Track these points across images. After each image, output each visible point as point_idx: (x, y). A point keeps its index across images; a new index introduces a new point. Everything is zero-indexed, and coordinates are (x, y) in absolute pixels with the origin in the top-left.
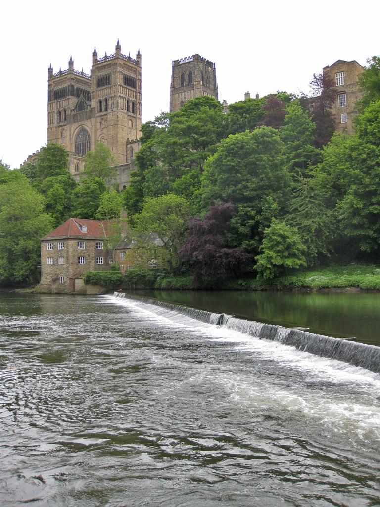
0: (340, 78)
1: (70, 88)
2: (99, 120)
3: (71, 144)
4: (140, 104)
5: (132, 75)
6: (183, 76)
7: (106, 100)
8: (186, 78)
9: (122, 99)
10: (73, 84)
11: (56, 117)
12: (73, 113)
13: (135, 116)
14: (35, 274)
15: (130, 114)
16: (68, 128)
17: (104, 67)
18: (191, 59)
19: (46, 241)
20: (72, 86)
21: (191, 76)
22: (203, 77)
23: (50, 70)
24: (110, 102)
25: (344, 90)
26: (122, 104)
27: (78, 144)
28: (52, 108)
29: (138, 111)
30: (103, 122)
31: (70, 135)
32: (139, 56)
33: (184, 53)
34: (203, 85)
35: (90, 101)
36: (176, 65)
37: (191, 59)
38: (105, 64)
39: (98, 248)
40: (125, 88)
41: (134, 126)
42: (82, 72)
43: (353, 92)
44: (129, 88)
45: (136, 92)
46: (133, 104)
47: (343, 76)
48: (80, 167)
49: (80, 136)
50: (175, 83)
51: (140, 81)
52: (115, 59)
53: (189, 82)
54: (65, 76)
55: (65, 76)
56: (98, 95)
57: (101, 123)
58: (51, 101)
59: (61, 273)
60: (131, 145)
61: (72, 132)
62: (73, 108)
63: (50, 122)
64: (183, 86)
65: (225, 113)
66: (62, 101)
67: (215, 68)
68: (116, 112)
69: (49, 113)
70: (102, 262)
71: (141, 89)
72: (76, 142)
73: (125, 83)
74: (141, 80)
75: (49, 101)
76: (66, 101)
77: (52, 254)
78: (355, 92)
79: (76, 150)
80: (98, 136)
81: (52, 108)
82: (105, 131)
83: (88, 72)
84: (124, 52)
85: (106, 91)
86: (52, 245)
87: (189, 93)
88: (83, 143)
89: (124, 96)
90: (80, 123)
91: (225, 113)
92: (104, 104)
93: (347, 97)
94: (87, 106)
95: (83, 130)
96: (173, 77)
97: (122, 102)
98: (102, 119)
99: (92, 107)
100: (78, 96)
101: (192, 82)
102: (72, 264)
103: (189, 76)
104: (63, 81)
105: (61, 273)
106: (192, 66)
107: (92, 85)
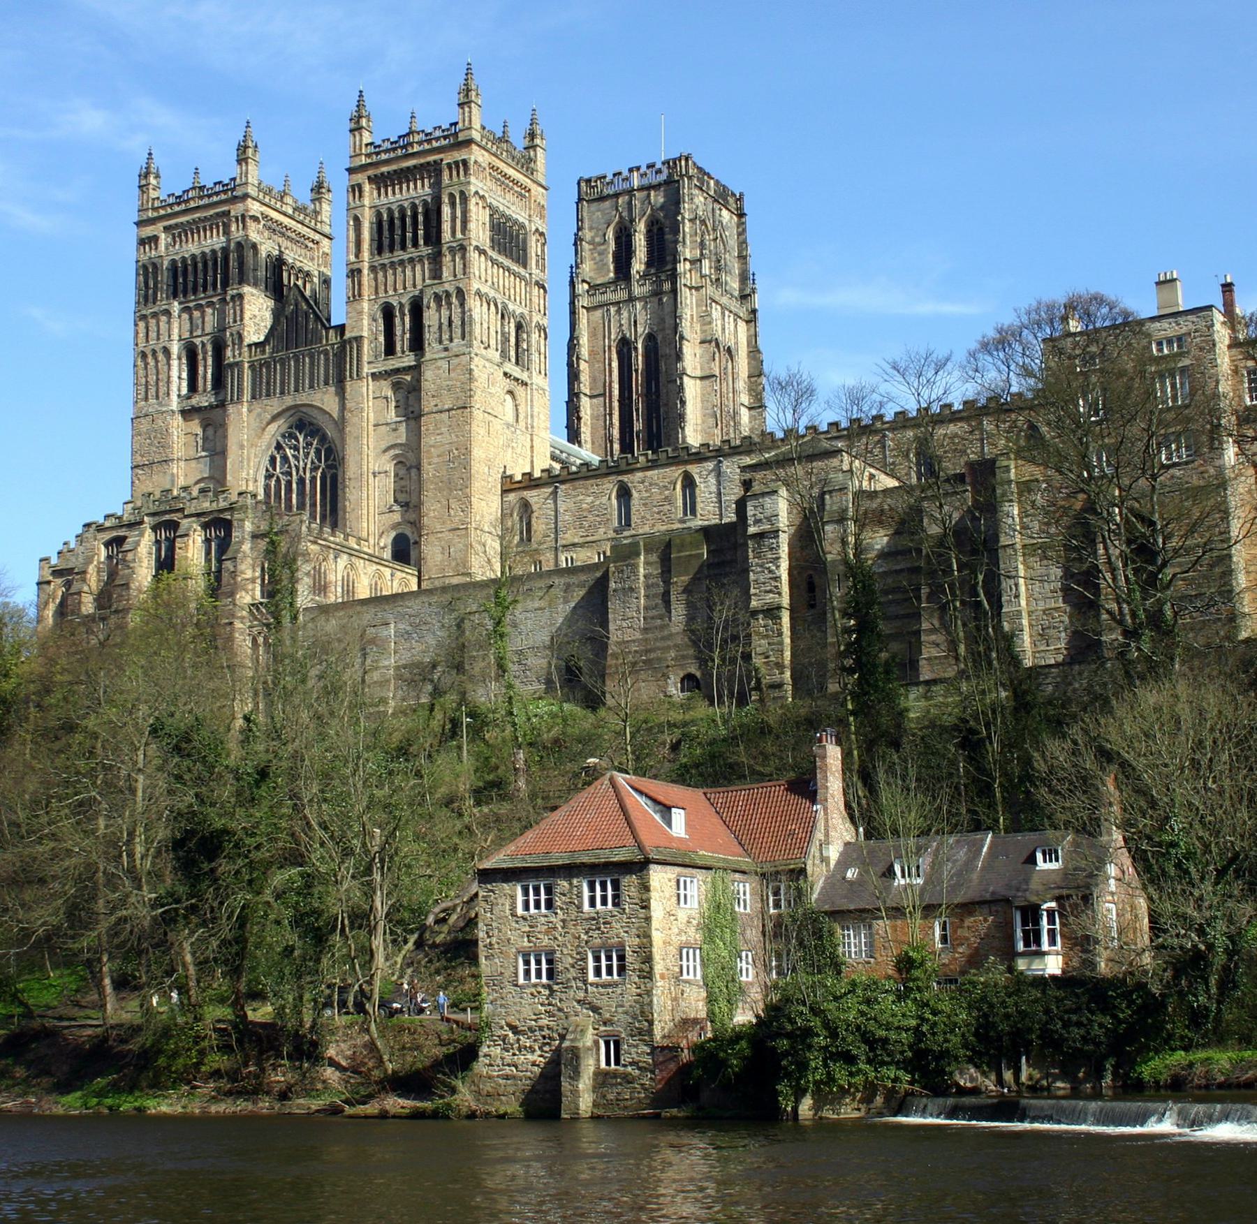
7: (417, 309)
9: (485, 305)
13: (524, 376)
18: (659, 171)
24: (431, 317)
26: (485, 326)
29: (535, 357)
37: (659, 171)
41: (521, 417)
44: (507, 262)
46: (519, 327)
68: (465, 359)
71: (543, 271)
72: (269, 476)
75: (138, 303)
81: (153, 335)
85: (418, 276)
88: (301, 481)
89: (492, 294)
92: (403, 326)
94: (327, 329)
97: (485, 317)
99: (348, 335)
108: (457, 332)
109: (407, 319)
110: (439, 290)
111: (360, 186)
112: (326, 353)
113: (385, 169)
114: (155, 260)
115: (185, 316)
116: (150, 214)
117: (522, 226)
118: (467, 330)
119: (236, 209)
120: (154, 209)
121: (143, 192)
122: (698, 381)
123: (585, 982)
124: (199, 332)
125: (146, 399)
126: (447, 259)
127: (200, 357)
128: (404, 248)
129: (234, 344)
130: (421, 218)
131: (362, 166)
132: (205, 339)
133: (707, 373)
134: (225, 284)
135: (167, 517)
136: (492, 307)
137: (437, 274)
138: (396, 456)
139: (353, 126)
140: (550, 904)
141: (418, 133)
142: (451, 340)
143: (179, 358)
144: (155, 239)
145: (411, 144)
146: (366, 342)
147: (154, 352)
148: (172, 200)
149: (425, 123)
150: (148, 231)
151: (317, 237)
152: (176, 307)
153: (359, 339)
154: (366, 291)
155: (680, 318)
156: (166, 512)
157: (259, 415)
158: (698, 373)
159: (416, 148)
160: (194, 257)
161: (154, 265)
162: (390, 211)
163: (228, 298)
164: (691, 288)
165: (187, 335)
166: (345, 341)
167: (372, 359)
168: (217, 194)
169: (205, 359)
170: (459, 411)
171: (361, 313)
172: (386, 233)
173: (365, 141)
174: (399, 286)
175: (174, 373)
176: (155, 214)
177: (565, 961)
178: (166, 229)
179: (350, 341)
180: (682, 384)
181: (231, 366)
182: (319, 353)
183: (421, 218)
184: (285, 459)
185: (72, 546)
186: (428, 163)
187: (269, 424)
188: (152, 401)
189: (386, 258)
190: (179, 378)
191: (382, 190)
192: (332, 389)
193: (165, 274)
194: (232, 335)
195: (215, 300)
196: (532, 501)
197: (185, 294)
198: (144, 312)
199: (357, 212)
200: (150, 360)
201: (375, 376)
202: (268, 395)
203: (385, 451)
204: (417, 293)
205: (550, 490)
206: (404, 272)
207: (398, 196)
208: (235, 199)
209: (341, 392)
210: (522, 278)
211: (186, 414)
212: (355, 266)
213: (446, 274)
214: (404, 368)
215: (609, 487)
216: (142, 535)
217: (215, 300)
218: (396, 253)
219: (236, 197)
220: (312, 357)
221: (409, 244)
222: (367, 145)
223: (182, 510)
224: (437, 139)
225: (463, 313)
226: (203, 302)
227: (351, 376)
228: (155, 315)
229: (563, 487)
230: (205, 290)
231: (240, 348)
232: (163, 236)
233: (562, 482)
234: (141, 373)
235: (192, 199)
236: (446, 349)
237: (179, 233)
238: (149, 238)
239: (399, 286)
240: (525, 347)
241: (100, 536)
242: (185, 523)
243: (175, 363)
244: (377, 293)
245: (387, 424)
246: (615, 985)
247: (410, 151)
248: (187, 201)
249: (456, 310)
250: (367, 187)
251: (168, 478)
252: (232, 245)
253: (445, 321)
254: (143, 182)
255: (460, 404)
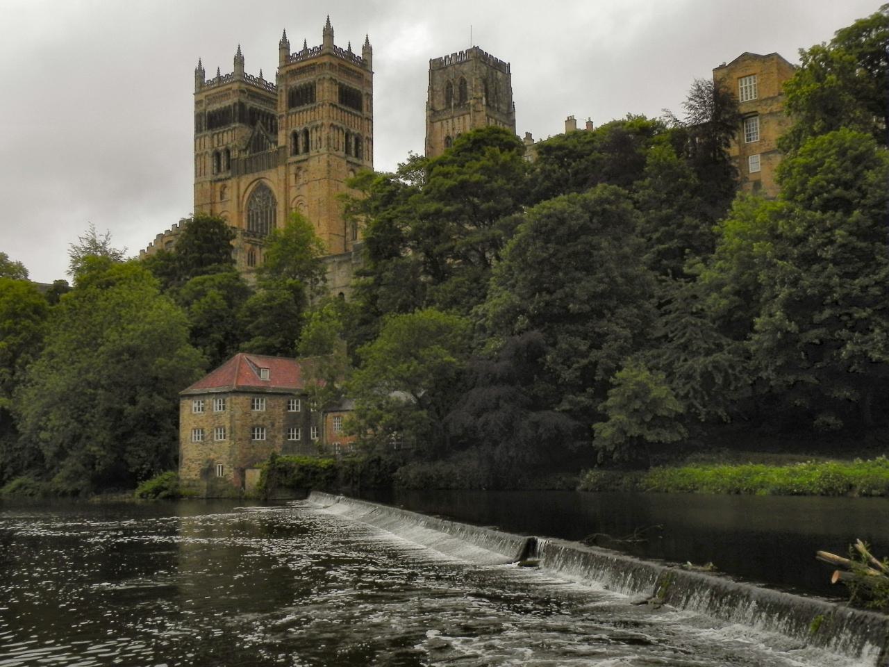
0: (746, 88)
1: (237, 108)
2: (293, 169)
3: (240, 213)
4: (371, 140)
5: (355, 85)
6: (449, 86)
7: (306, 133)
8: (455, 90)
9: (336, 131)
10: (243, 100)
11: (209, 162)
12: (243, 156)
13: (360, 162)
14: (170, 458)
15: (350, 159)
16: (235, 184)
17: (302, 70)
18: (465, 55)
19: (191, 396)
20: (242, 105)
21: (466, 88)
22: (486, 91)
23: (200, 73)
24: (314, 137)
25: (754, 110)
27: (253, 215)
28: (202, 146)
29: (365, 153)
30: (301, 173)
31: (238, 197)
32: (367, 49)
33: (451, 44)
34: (488, 105)
35: (276, 133)
36: (437, 67)
38: (304, 64)
39: (292, 410)
40: (342, 110)
42: (261, 78)
43: (771, 113)
44: (349, 109)
45: (361, 119)
46: (357, 141)
47: (753, 83)
48: (258, 258)
49: (257, 199)
50: (435, 101)
51: (370, 96)
52: (323, 55)
53: (461, 100)
54: (230, 86)
55: (230, 86)
56: (291, 122)
57: (296, 175)
58: (201, 131)
59: (218, 458)
61: (242, 191)
62: (244, 147)
63: (199, 173)
64: (450, 107)
65: (530, 157)
66: (224, 132)
67: (509, 74)
69: (196, 156)
70: (297, 436)
71: (372, 111)
72: (249, 211)
73: (341, 101)
74: (371, 96)
76: (230, 133)
77: (201, 421)
78: (776, 113)
79: (249, 227)
80: (291, 199)
81: (202, 146)
82: (304, 190)
83: (270, 77)
84: (340, 42)
86: (201, 404)
87: (461, 120)
88: (262, 213)
89: (340, 125)
90: (256, 175)
91: (530, 157)
92: (301, 140)
93: (761, 123)
95: (262, 188)
96: (431, 89)
97: (336, 136)
98: (299, 168)
99: (279, 145)
100: (253, 123)
101: (467, 100)
102: (240, 439)
103: (460, 88)
104: (225, 95)
105: (218, 458)
106: (465, 69)
107: (279, 103)
110: (315, 124)
117: (359, 92)
123: (212, 440)
136: (341, 131)
140: (224, 408)
165: (216, 145)
177: (207, 433)
188: (203, 176)
189: (293, 110)
210: (358, 116)
246: (221, 442)
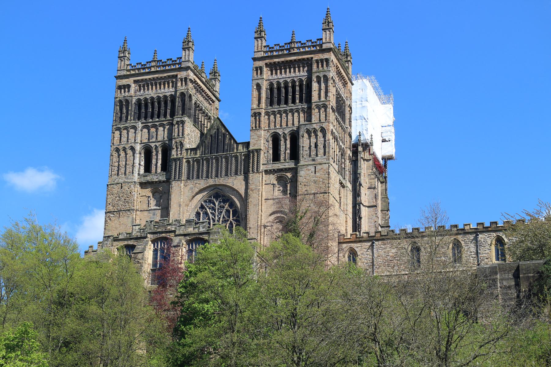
7: (295, 137)
24: (304, 142)
31: (180, 206)
60: (354, 245)
81: (124, 139)
85: (298, 119)
99: (251, 148)
108: (321, 151)
109: (288, 142)
111: (261, 68)
112: (236, 157)
113: (276, 60)
114: (128, 98)
115: (145, 130)
116: (125, 73)
118: (327, 150)
119: (182, 75)
120: (128, 70)
121: (122, 61)
122: (367, 208)
124: (154, 140)
125: (118, 174)
126: (315, 112)
127: (154, 153)
128: (286, 103)
129: (177, 148)
130: (298, 88)
131: (262, 57)
132: (158, 144)
133: (372, 204)
134: (173, 115)
135: (164, 235)
137: (309, 119)
138: (278, 217)
139: (256, 35)
141: (297, 42)
142: (317, 155)
143: (140, 154)
144: (129, 86)
145: (293, 48)
146: (262, 153)
147: (124, 149)
148: (139, 66)
149: (301, 37)
150: (124, 82)
151: (214, 99)
152: (140, 125)
153: (258, 151)
154: (262, 126)
155: (360, 174)
156: (162, 232)
157: (191, 189)
158: (367, 204)
159: (296, 51)
160: (152, 98)
161: (127, 101)
162: (279, 83)
163: (175, 122)
164: (364, 160)
165: (146, 141)
166: (249, 151)
167: (266, 162)
168: (169, 65)
169: (157, 155)
170: (322, 195)
171: (259, 136)
172: (275, 95)
173: (264, 44)
174: (284, 125)
175: (137, 161)
176: (128, 73)
178: (135, 82)
179: (253, 151)
180: (360, 208)
181: (175, 160)
182: (232, 157)
183: (298, 88)
184: (206, 214)
185: (95, 248)
186: (303, 59)
187: (197, 194)
189: (276, 108)
190: (140, 164)
191: (274, 72)
192: (242, 177)
193: (134, 106)
194: (176, 142)
195: (165, 123)
196: (357, 249)
197: (146, 118)
198: (119, 126)
199: (259, 81)
200: (122, 154)
201: (267, 172)
202: (198, 177)
203: (270, 215)
204: (295, 129)
205: (370, 244)
206: (287, 116)
207: (284, 75)
208: (181, 69)
209: (246, 179)
211: (143, 185)
212: (257, 111)
213: (315, 119)
214: (286, 169)
215: (406, 245)
216: (147, 244)
217: (165, 123)
218: (281, 106)
219: (182, 68)
220: (227, 159)
221: (290, 101)
222: (265, 47)
223: (174, 232)
224: (309, 47)
225: (325, 141)
226: (157, 124)
227: (253, 171)
228: (126, 128)
229: (377, 243)
230: (158, 117)
231: (181, 150)
232: (133, 85)
233: (378, 240)
234: (115, 159)
235: (153, 66)
236: (314, 160)
237: (143, 84)
238: (124, 85)
239: (284, 125)
240: (343, 167)
241: (115, 243)
242: (176, 241)
243: (137, 156)
244: (269, 127)
245: (273, 199)
247: (292, 51)
248: (150, 68)
249: (321, 140)
250: (265, 69)
251: (130, 220)
252: (178, 94)
253: (313, 145)
254: (122, 55)
255: (322, 191)
